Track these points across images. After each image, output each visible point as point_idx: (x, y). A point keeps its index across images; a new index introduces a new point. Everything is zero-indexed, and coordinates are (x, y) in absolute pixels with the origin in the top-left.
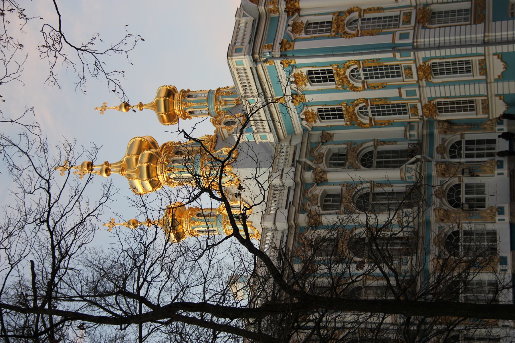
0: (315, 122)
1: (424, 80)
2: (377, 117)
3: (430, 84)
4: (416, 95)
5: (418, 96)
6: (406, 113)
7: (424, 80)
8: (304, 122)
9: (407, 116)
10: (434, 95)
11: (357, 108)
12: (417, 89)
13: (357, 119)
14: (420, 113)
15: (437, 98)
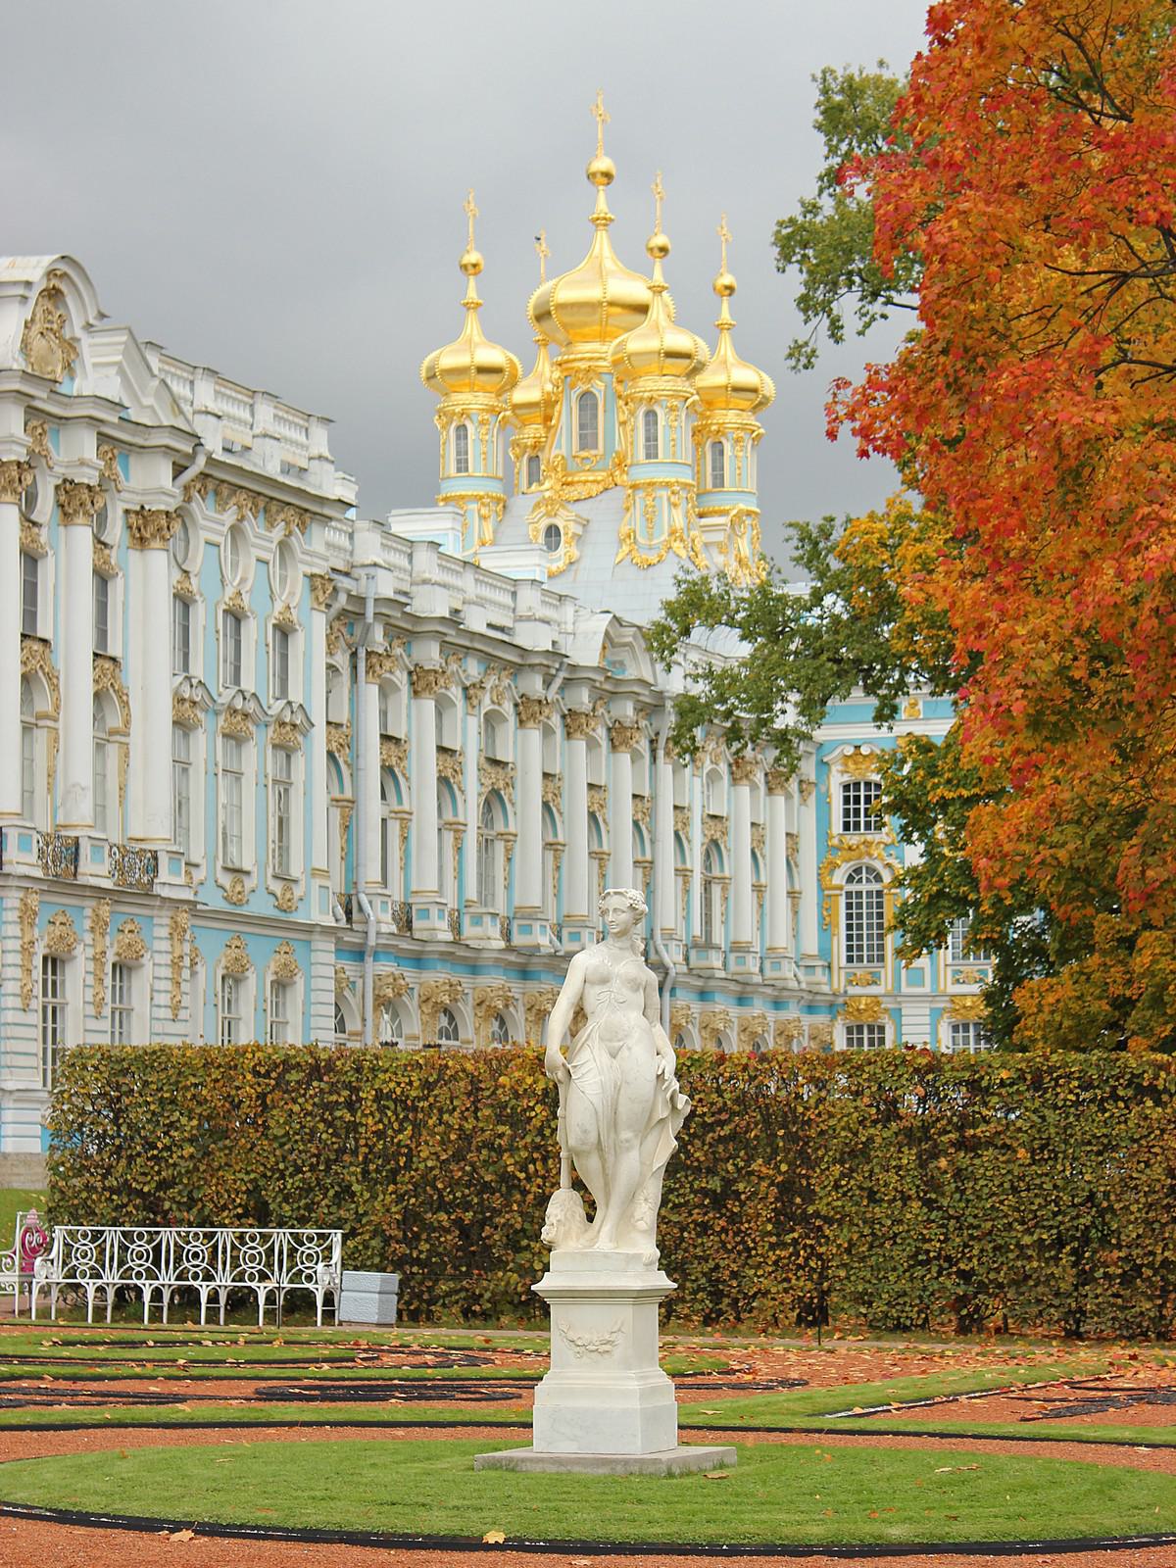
0: (843, 773)
1: (948, 1005)
2: (843, 901)
3: (936, 1015)
4: (909, 984)
5: (905, 990)
6: (850, 959)
7: (948, 1005)
8: (850, 751)
9: (843, 962)
10: (904, 1020)
11: (878, 865)
12: (927, 989)
13: (848, 861)
14: (851, 991)
15: (899, 1026)
